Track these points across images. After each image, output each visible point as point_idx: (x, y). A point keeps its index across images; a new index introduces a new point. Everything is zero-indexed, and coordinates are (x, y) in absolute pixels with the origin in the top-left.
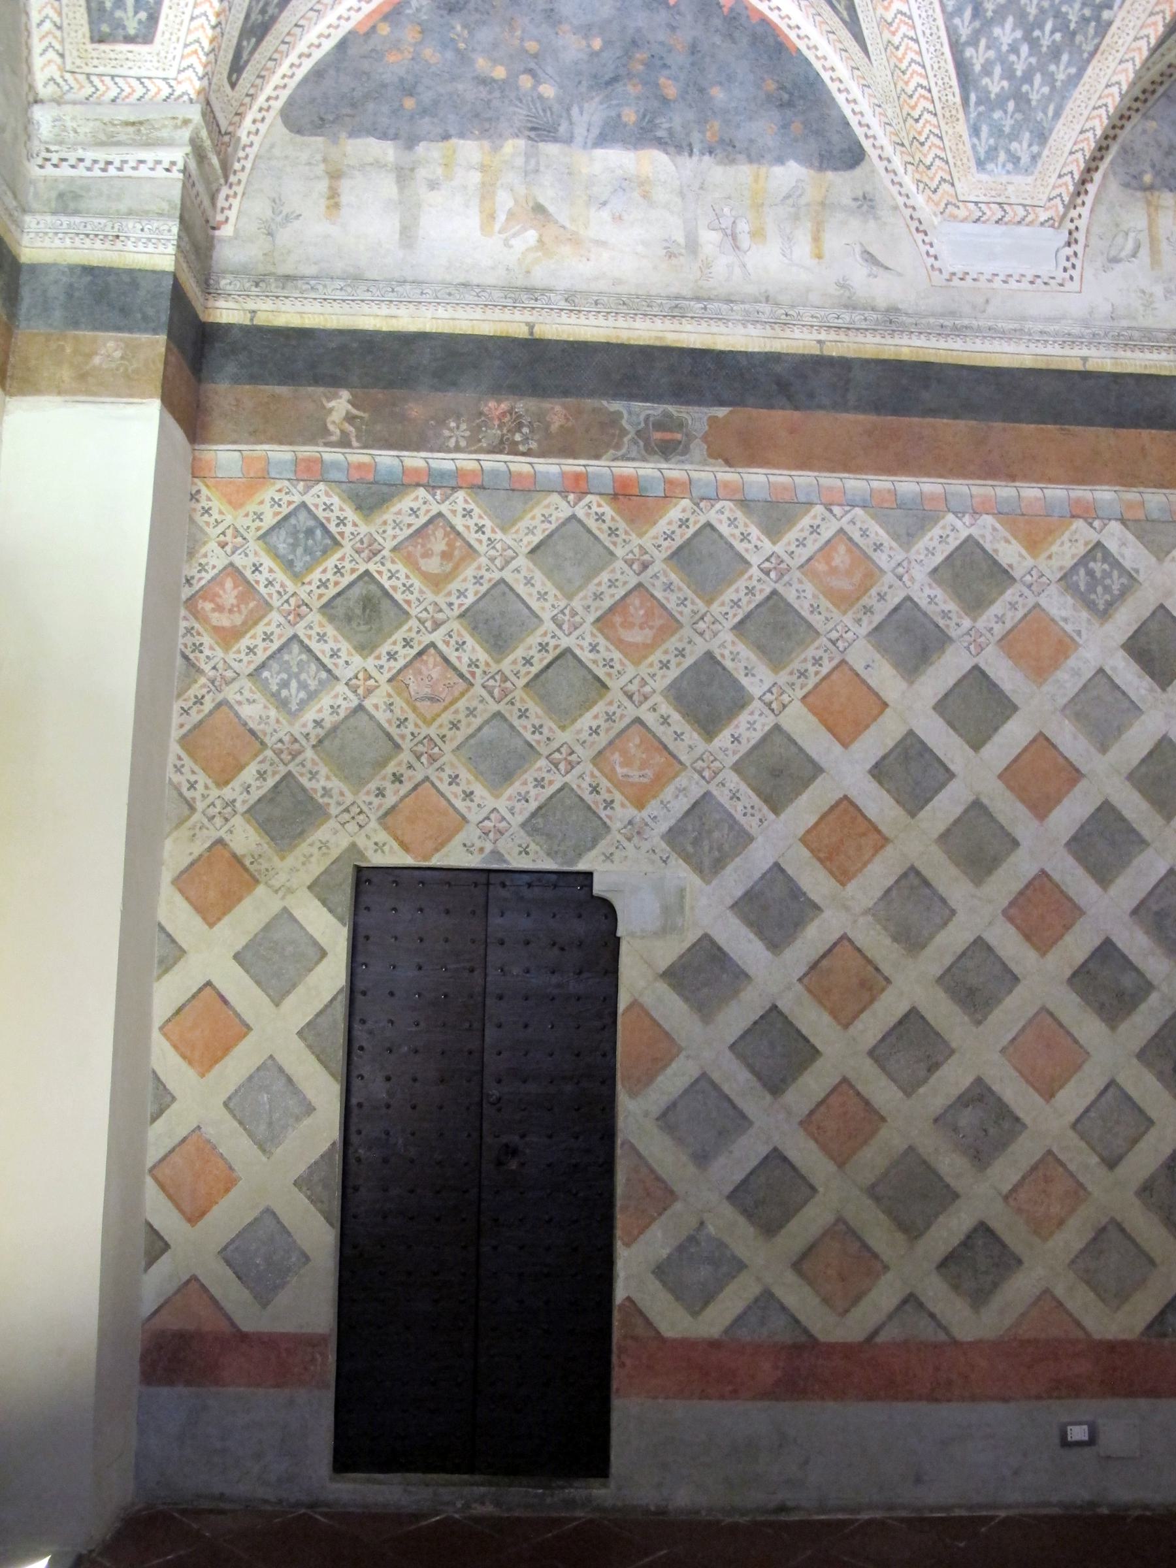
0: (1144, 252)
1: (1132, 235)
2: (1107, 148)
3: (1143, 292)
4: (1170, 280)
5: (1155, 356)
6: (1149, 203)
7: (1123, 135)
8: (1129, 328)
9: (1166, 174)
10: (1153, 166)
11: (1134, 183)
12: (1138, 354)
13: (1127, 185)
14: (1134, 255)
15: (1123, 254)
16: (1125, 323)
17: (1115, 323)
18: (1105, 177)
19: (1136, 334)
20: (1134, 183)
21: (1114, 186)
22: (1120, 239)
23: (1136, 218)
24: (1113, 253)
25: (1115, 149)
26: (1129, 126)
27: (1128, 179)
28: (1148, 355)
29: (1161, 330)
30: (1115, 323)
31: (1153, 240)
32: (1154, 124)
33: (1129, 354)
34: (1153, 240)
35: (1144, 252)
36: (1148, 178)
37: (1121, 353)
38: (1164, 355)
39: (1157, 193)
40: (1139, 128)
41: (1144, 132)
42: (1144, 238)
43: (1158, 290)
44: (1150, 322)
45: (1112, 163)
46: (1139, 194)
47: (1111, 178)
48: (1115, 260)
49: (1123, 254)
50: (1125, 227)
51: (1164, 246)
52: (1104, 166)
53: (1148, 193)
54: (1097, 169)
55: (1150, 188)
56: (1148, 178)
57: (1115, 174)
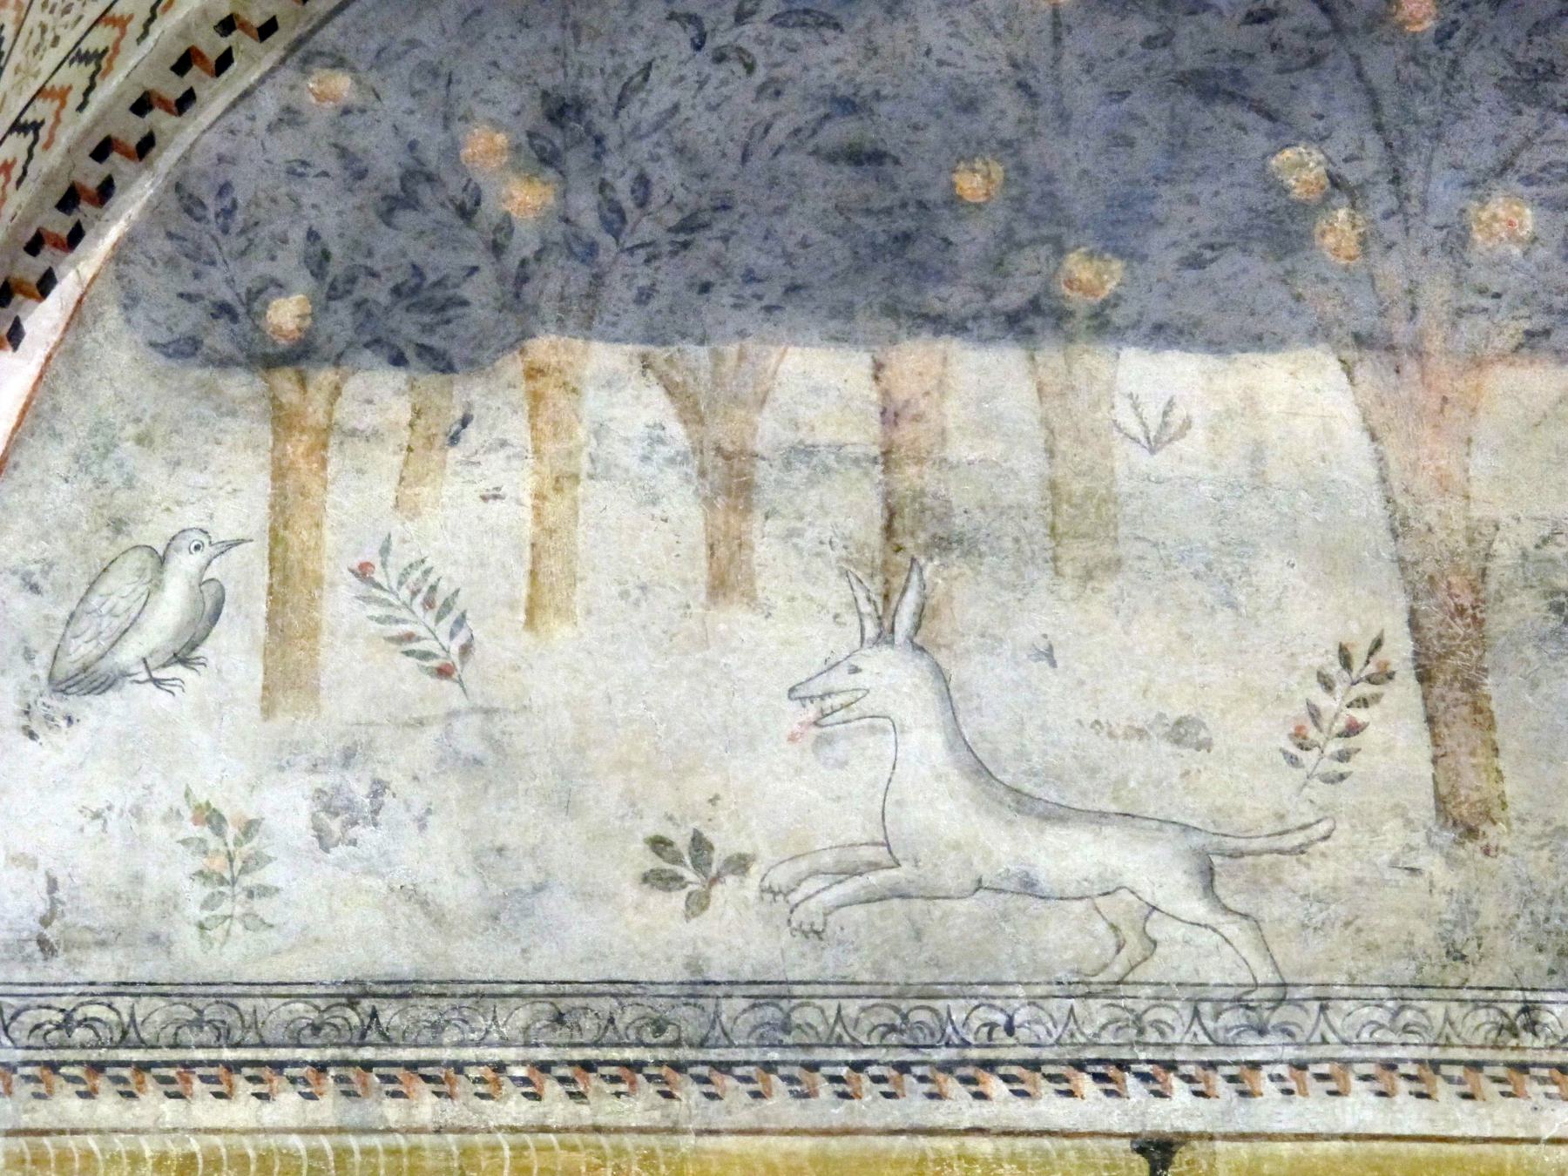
0: (235, 650)
1: (185, 565)
2: (106, 191)
3: (212, 818)
4: (348, 757)
5: (242, 1110)
6: (283, 420)
7: (183, 138)
8: (123, 987)
9: (379, 293)
10: (319, 262)
11: (219, 338)
12: (154, 1107)
13: (185, 349)
14: (184, 656)
15: (128, 654)
16: (102, 967)
17: (56, 970)
18: (78, 317)
19: (155, 1014)
20: (222, 339)
21: (119, 355)
22: (122, 587)
23: (216, 488)
24: (81, 650)
25: (139, 194)
26: (216, 97)
27: (190, 318)
28: (204, 1109)
29: (284, 989)
30: (56, 970)
31: (289, 580)
32: (342, 84)
33: (107, 1108)
34: (289, 580)
35: (235, 650)
36: (286, 314)
37: (68, 1106)
38: (287, 1106)
39: (325, 377)
40: (268, 104)
41: (290, 117)
42: (247, 574)
43: (287, 808)
44: (232, 956)
45: (119, 255)
46: (238, 384)
47: (112, 316)
48: (94, 680)
49: (128, 654)
50: (154, 532)
51: (341, 605)
52: (77, 273)
53: (284, 381)
54: (46, 284)
55: (298, 355)
56: (286, 314)
57: (130, 302)
